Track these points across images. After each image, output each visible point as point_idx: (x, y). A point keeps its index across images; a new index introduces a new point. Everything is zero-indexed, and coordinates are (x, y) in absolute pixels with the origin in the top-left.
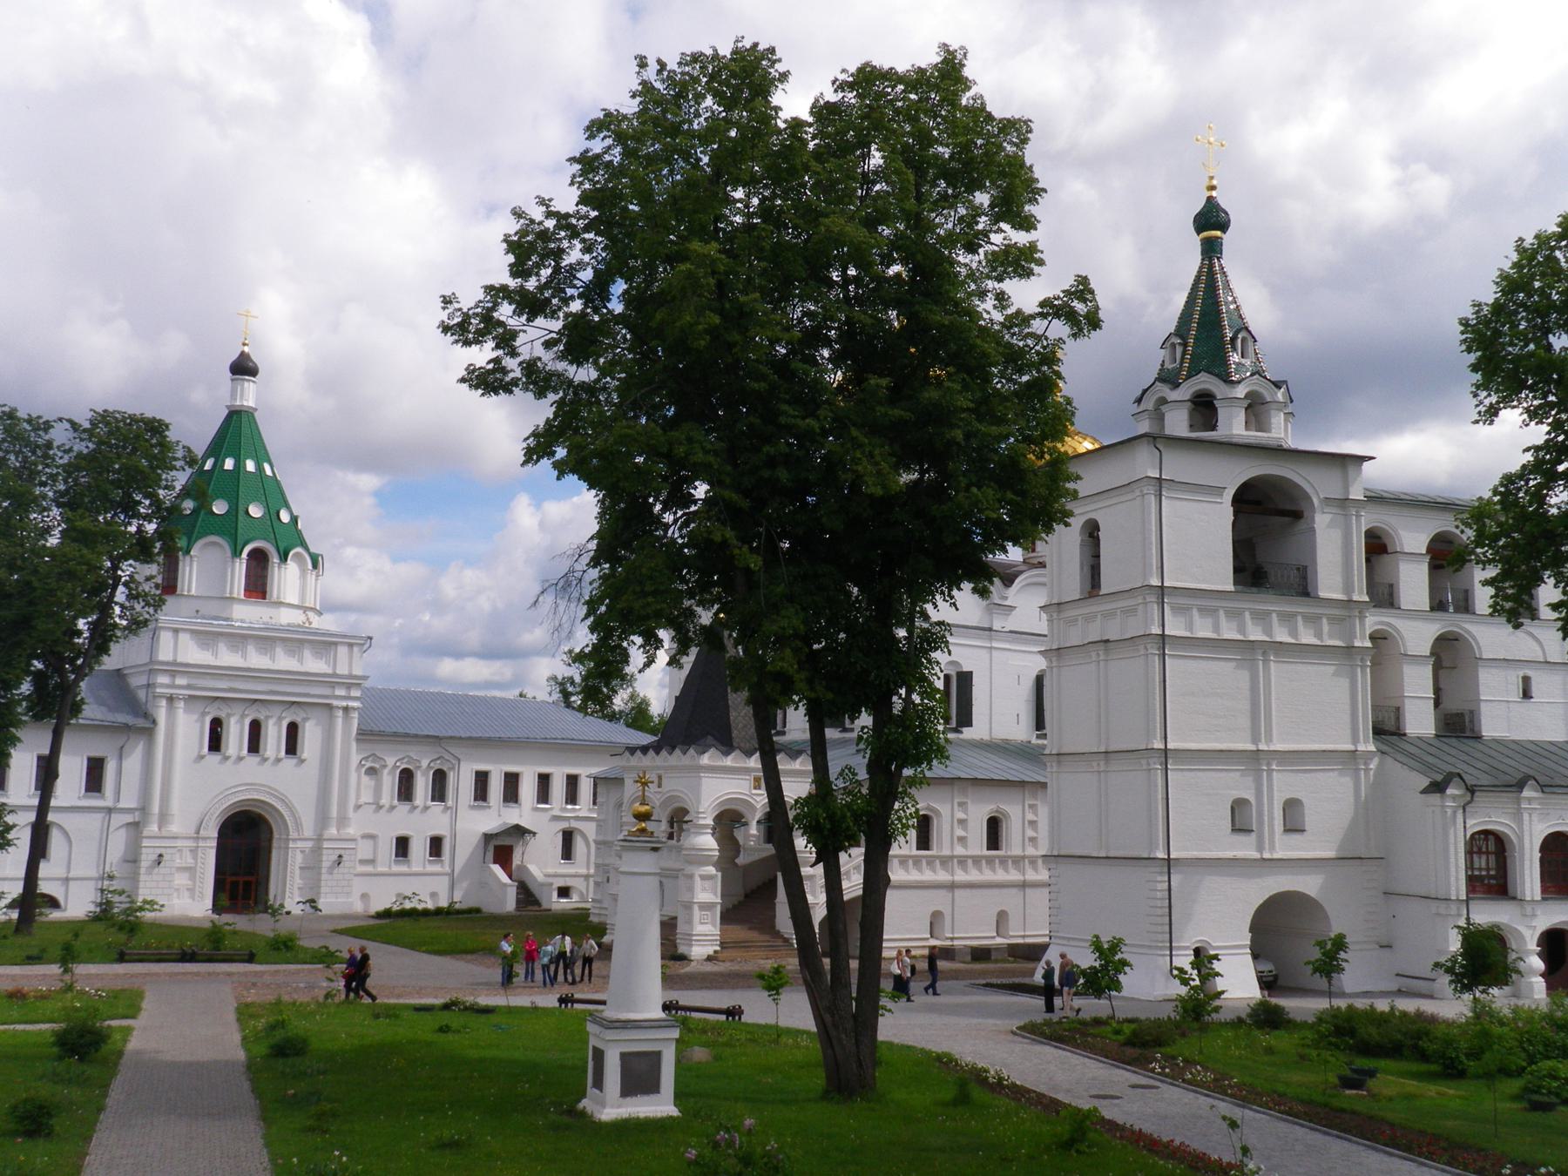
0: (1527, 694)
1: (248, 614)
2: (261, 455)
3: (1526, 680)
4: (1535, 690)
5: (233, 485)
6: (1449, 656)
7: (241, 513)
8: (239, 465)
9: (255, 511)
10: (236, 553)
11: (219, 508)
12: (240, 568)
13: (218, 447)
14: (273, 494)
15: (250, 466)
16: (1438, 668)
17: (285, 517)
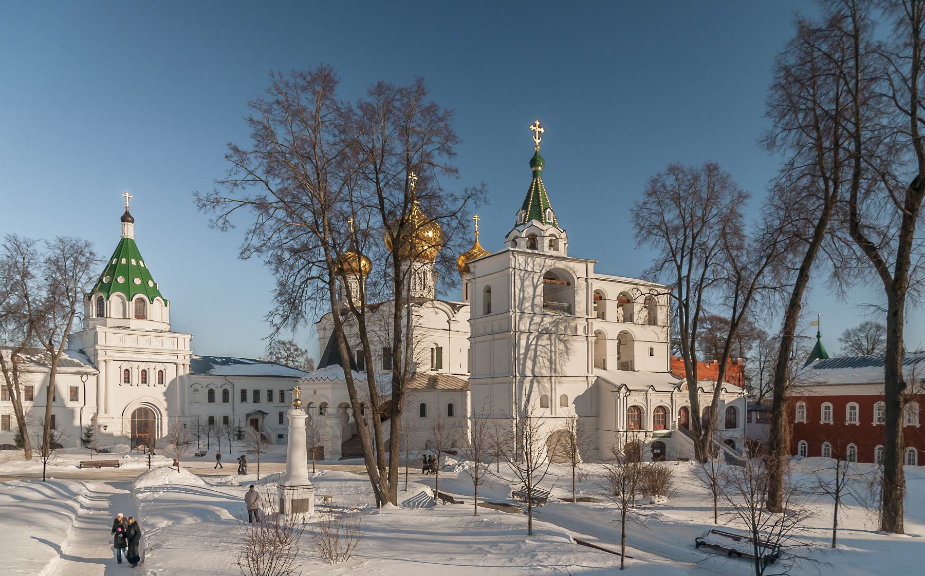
0: (651, 355)
1: (135, 324)
2: (138, 258)
3: (651, 349)
4: (654, 354)
5: (127, 271)
6: (624, 340)
7: (131, 282)
8: (128, 261)
9: (137, 281)
10: (130, 300)
11: (121, 280)
12: (131, 306)
13: (118, 254)
14: (145, 275)
15: (133, 262)
16: (619, 344)
17: (151, 284)
